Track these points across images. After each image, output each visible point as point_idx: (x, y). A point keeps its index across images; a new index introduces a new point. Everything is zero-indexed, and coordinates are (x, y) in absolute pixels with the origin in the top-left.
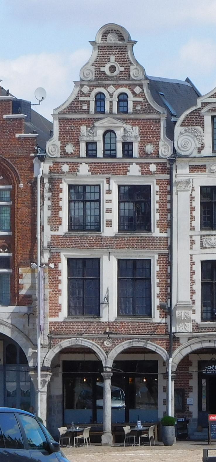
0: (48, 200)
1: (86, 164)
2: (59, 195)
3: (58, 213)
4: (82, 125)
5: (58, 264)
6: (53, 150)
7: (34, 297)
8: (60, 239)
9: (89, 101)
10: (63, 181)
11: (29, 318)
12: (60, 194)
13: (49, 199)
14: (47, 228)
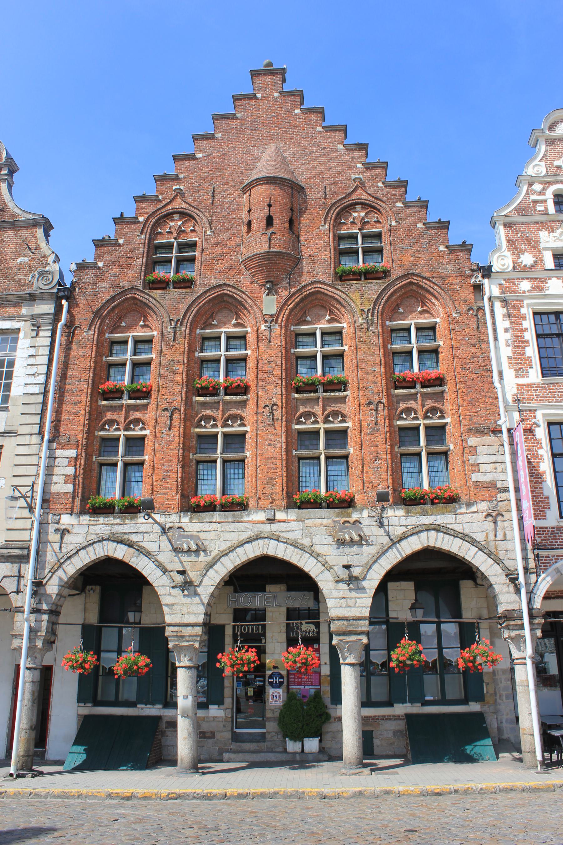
0: (505, 332)
1: (558, 279)
2: (522, 324)
3: (524, 351)
4: (541, 230)
5: (535, 430)
6: (503, 262)
7: (499, 485)
8: (534, 390)
9: (545, 201)
10: (525, 305)
11: (495, 522)
12: (524, 322)
13: (506, 330)
14: (509, 374)
